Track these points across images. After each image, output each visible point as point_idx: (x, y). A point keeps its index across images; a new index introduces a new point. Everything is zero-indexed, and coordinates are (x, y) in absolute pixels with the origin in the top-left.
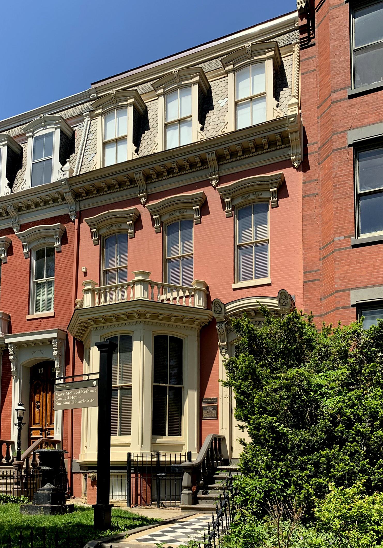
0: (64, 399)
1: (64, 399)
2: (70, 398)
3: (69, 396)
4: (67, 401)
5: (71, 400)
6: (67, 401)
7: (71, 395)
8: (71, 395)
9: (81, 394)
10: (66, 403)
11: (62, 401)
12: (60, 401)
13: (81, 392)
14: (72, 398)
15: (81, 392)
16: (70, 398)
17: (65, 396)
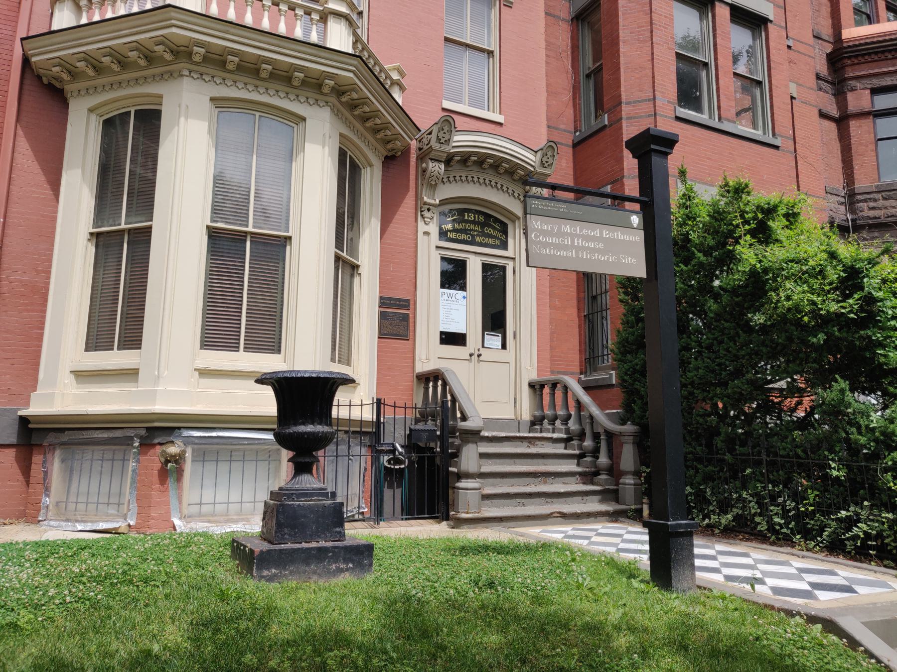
0: (556, 240)
1: (556, 240)
2: (573, 241)
3: (573, 236)
4: (565, 248)
5: (578, 249)
6: (565, 248)
7: (578, 236)
8: (578, 236)
9: (600, 239)
10: (563, 253)
11: (552, 244)
12: (545, 245)
13: (601, 233)
14: (579, 242)
15: (601, 233)
16: (573, 241)
17: (561, 234)
